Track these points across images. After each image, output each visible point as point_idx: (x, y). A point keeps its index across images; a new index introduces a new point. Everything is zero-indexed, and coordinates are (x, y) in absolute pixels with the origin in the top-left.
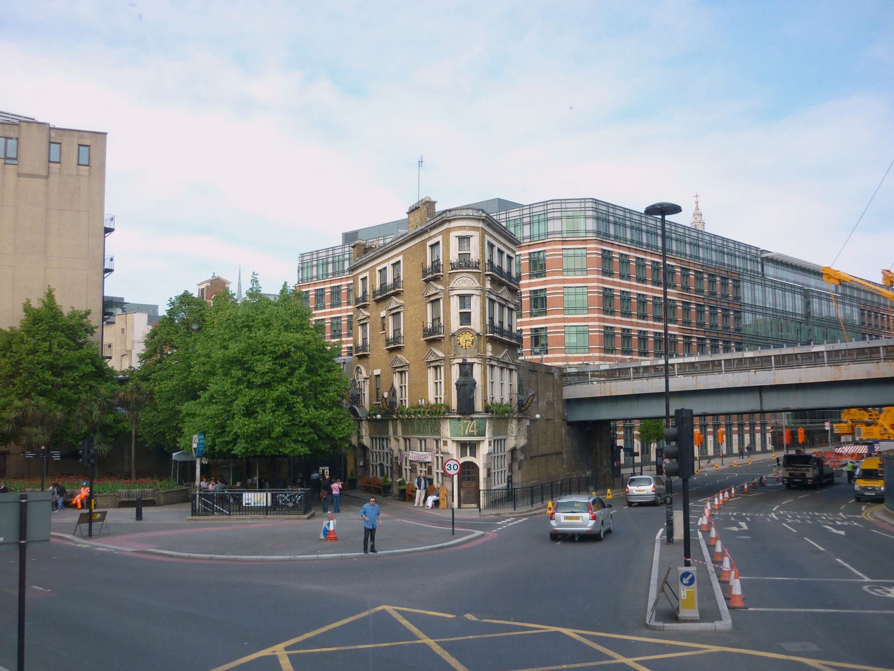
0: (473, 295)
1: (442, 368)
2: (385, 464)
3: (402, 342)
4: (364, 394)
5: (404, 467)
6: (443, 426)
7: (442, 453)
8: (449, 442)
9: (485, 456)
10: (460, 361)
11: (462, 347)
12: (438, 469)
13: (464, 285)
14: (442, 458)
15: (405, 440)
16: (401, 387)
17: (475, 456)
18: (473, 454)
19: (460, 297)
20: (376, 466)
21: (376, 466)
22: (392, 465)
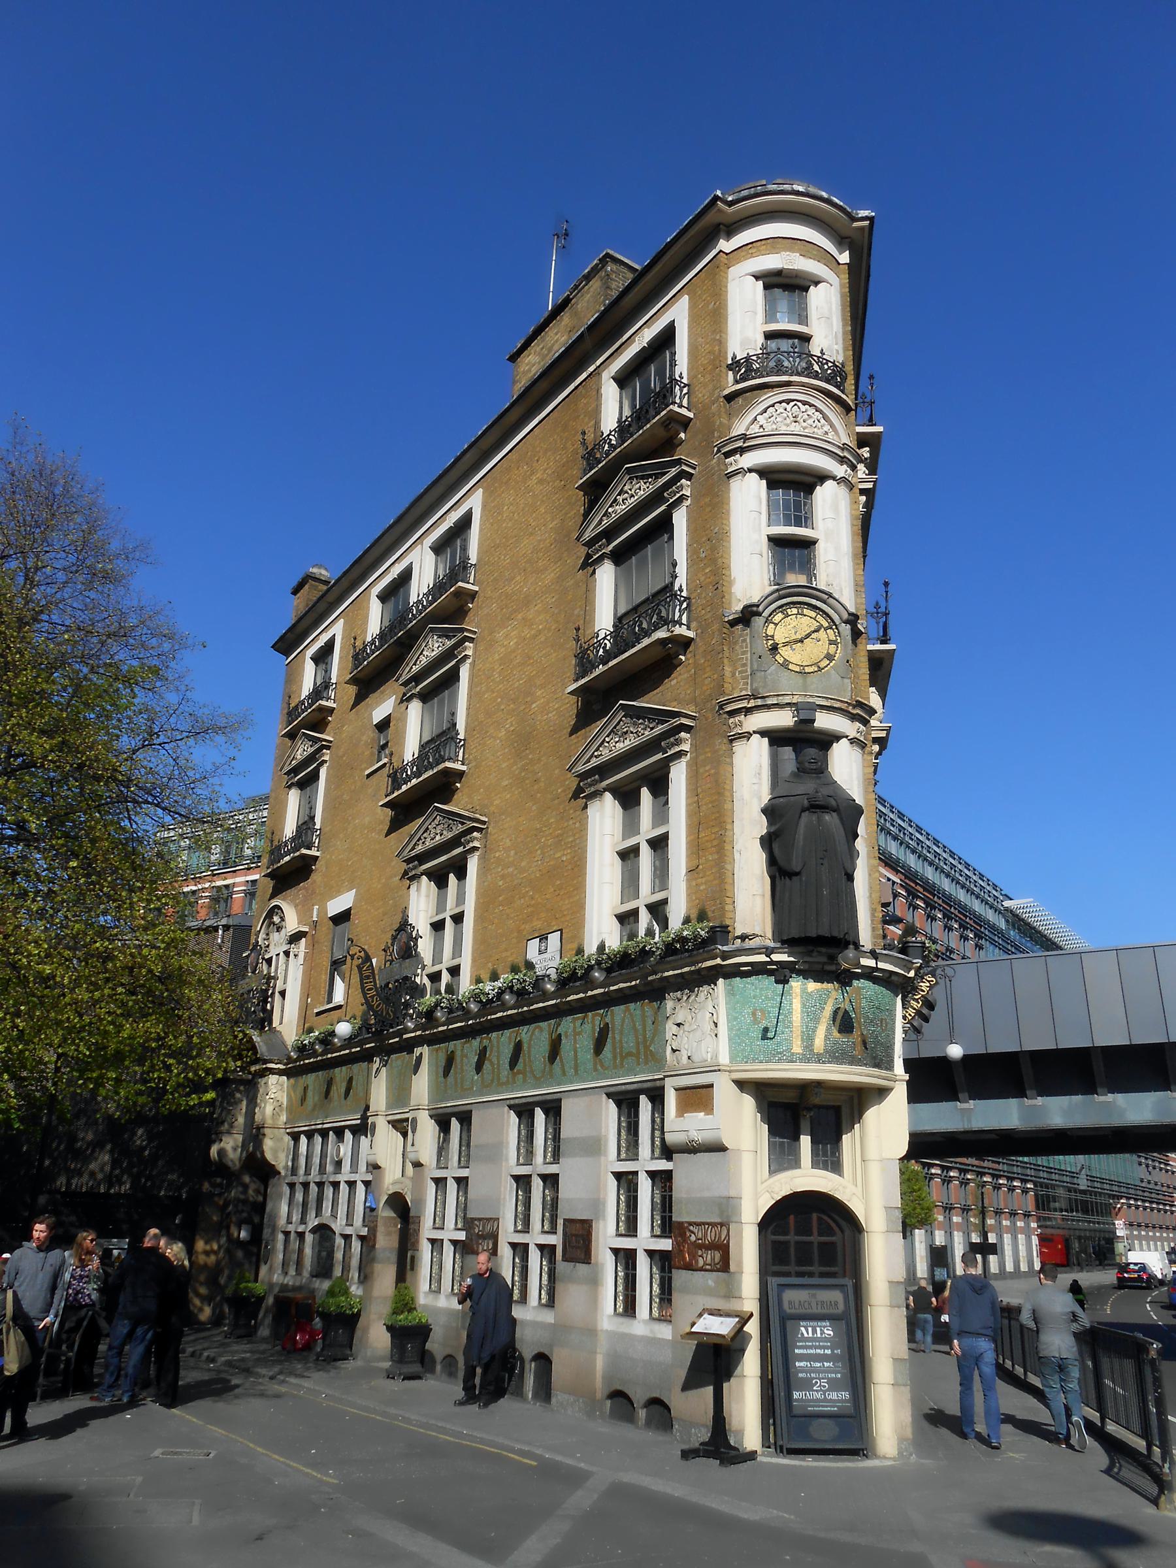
0: (823, 477)
1: (679, 775)
2: (338, 1226)
3: (460, 758)
4: (283, 994)
5: (427, 1230)
6: (681, 1015)
7: (667, 1152)
8: (725, 1092)
9: (896, 1168)
10: (784, 719)
11: (785, 665)
12: (631, 1227)
13: (794, 427)
14: (662, 1179)
15: (443, 1122)
16: (438, 926)
17: (836, 1166)
18: (828, 1157)
19: (771, 486)
20: (301, 1235)
21: (301, 1235)
22: (373, 1231)
